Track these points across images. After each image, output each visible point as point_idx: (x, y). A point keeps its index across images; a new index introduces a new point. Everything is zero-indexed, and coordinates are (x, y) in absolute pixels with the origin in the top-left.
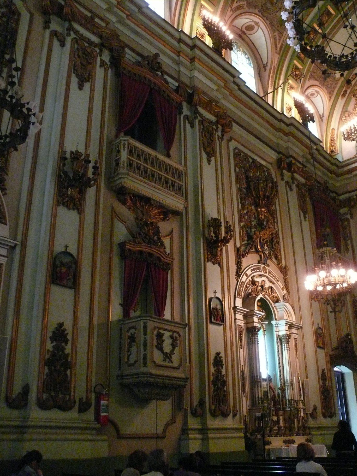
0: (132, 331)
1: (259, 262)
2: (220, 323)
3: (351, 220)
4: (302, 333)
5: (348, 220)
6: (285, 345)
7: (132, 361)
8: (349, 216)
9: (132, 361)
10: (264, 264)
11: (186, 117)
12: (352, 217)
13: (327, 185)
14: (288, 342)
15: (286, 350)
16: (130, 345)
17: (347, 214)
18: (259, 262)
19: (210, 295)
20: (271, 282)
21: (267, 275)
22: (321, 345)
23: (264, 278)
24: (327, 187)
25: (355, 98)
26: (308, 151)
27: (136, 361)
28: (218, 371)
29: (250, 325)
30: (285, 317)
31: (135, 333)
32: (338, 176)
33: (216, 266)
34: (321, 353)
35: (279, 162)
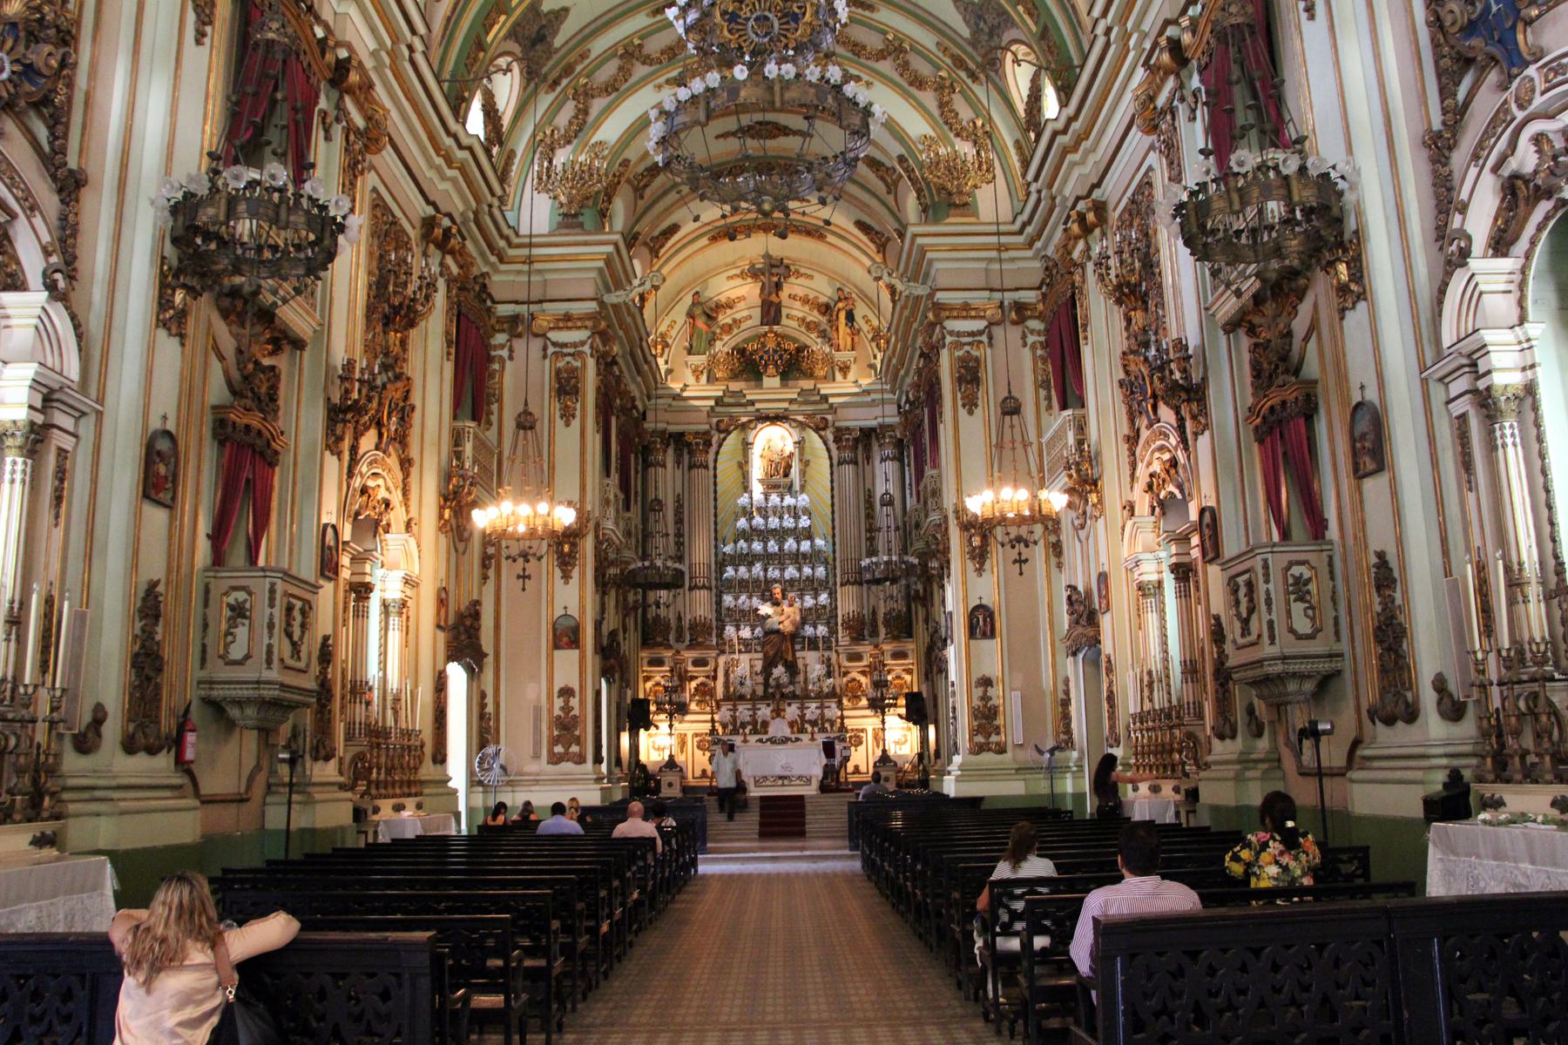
0: (241, 596)
1: (377, 448)
2: (331, 575)
3: (508, 364)
4: (418, 594)
5: (502, 360)
6: (394, 621)
7: (237, 652)
8: (505, 353)
9: (237, 652)
10: (384, 452)
11: (324, 114)
12: (511, 358)
13: (487, 281)
14: (401, 614)
15: (397, 632)
16: (233, 623)
17: (502, 347)
18: (377, 448)
19: (325, 520)
20: (388, 489)
21: (384, 474)
22: (442, 624)
23: (380, 482)
24: (484, 286)
25: (575, 103)
26: (474, 204)
27: (248, 657)
28: (324, 672)
29: (357, 579)
30: (403, 564)
31: (245, 601)
32: (501, 261)
33: (335, 457)
34: (441, 635)
35: (429, 224)
